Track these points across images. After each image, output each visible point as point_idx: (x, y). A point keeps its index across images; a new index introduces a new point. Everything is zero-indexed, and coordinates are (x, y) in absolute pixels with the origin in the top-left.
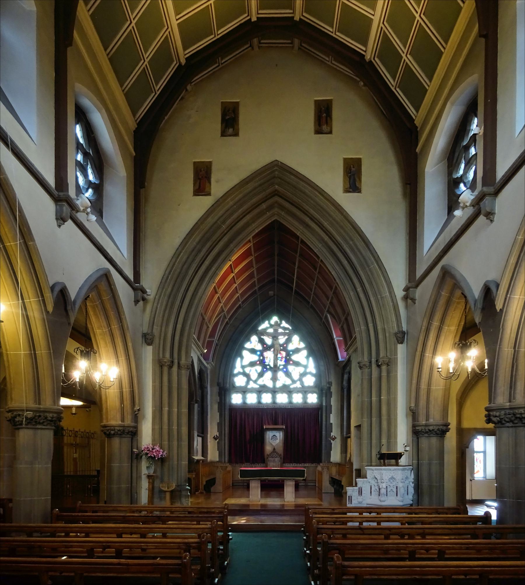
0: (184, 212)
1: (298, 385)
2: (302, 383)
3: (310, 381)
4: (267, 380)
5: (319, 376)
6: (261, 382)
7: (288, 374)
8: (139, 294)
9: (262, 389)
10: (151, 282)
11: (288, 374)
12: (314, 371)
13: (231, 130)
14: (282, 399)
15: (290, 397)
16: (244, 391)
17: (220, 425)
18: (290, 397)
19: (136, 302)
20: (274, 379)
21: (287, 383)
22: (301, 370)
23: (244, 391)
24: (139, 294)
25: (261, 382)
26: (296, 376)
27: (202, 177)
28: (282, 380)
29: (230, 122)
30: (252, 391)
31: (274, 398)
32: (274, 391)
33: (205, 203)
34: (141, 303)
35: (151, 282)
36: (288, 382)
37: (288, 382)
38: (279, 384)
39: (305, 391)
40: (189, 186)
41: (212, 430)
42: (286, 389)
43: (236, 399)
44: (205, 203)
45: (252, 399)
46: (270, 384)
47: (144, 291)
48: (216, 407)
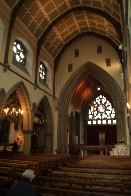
0: (66, 76)
1: (109, 117)
2: (111, 116)
3: (113, 116)
4: (99, 116)
5: (116, 114)
6: (97, 117)
7: (106, 114)
8: (55, 98)
9: (98, 119)
10: (57, 95)
11: (106, 114)
12: (114, 113)
13: (77, 56)
14: (104, 122)
15: (107, 122)
16: (92, 120)
17: (84, 132)
18: (107, 122)
19: (54, 100)
20: (101, 115)
21: (106, 117)
22: (110, 112)
23: (92, 120)
24: (55, 98)
25: (97, 117)
26: (109, 115)
27: (70, 67)
28: (104, 116)
29: (77, 54)
30: (94, 120)
31: (102, 122)
32: (102, 120)
33: (71, 73)
34: (55, 100)
35: (57, 95)
36: (106, 116)
37: (106, 116)
38: (103, 118)
39: (112, 119)
40: (67, 69)
41: (81, 133)
42: (105, 119)
43: (89, 123)
44: (71, 73)
45: (94, 122)
46: (100, 118)
47: (55, 97)
48: (83, 126)
